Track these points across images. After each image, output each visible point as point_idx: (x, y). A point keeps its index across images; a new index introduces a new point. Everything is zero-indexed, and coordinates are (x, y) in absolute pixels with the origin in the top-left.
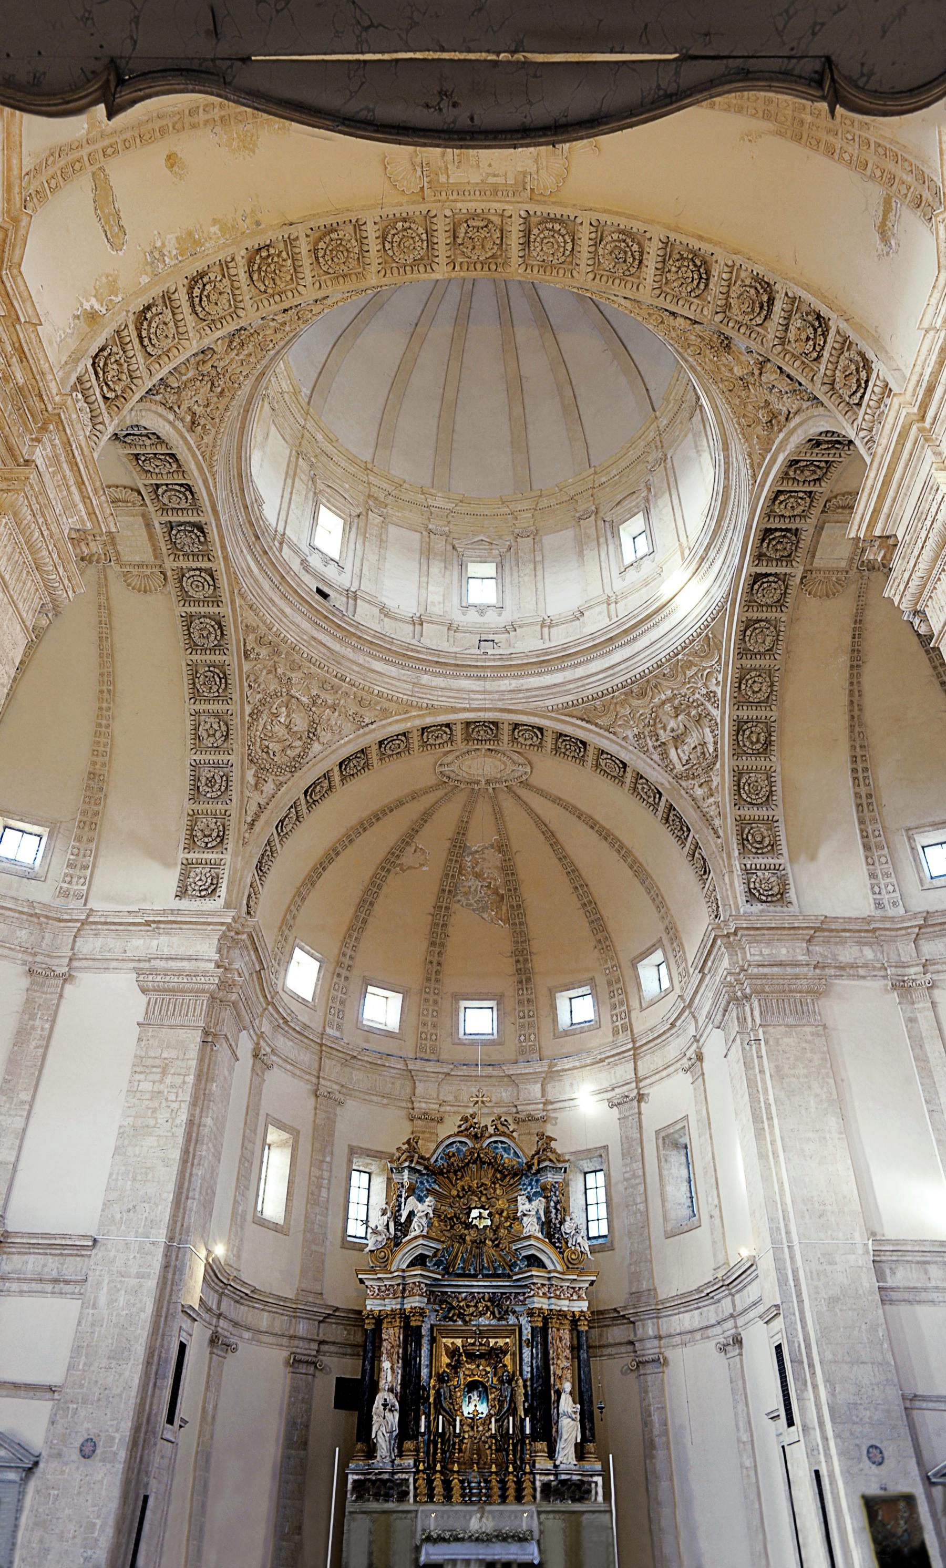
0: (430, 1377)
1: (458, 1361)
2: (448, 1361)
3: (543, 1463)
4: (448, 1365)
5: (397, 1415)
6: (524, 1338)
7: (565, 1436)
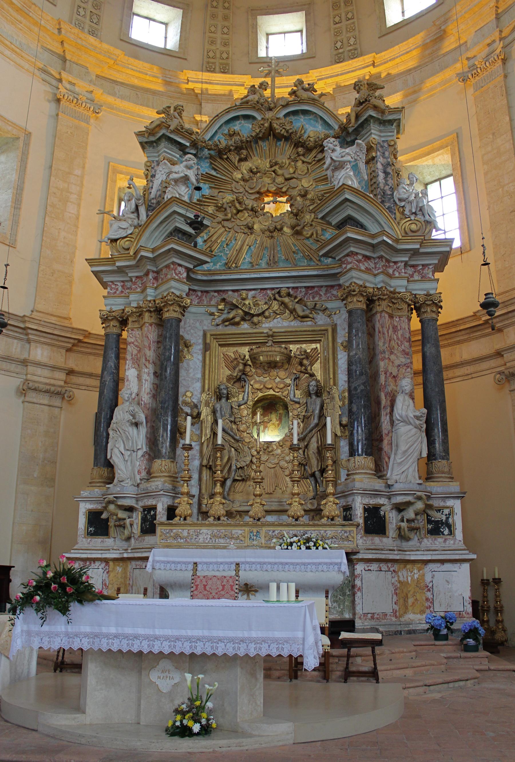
0: (203, 391)
1: (244, 373)
2: (228, 372)
3: (364, 481)
4: (229, 378)
5: (143, 430)
6: (339, 340)
7: (403, 448)
